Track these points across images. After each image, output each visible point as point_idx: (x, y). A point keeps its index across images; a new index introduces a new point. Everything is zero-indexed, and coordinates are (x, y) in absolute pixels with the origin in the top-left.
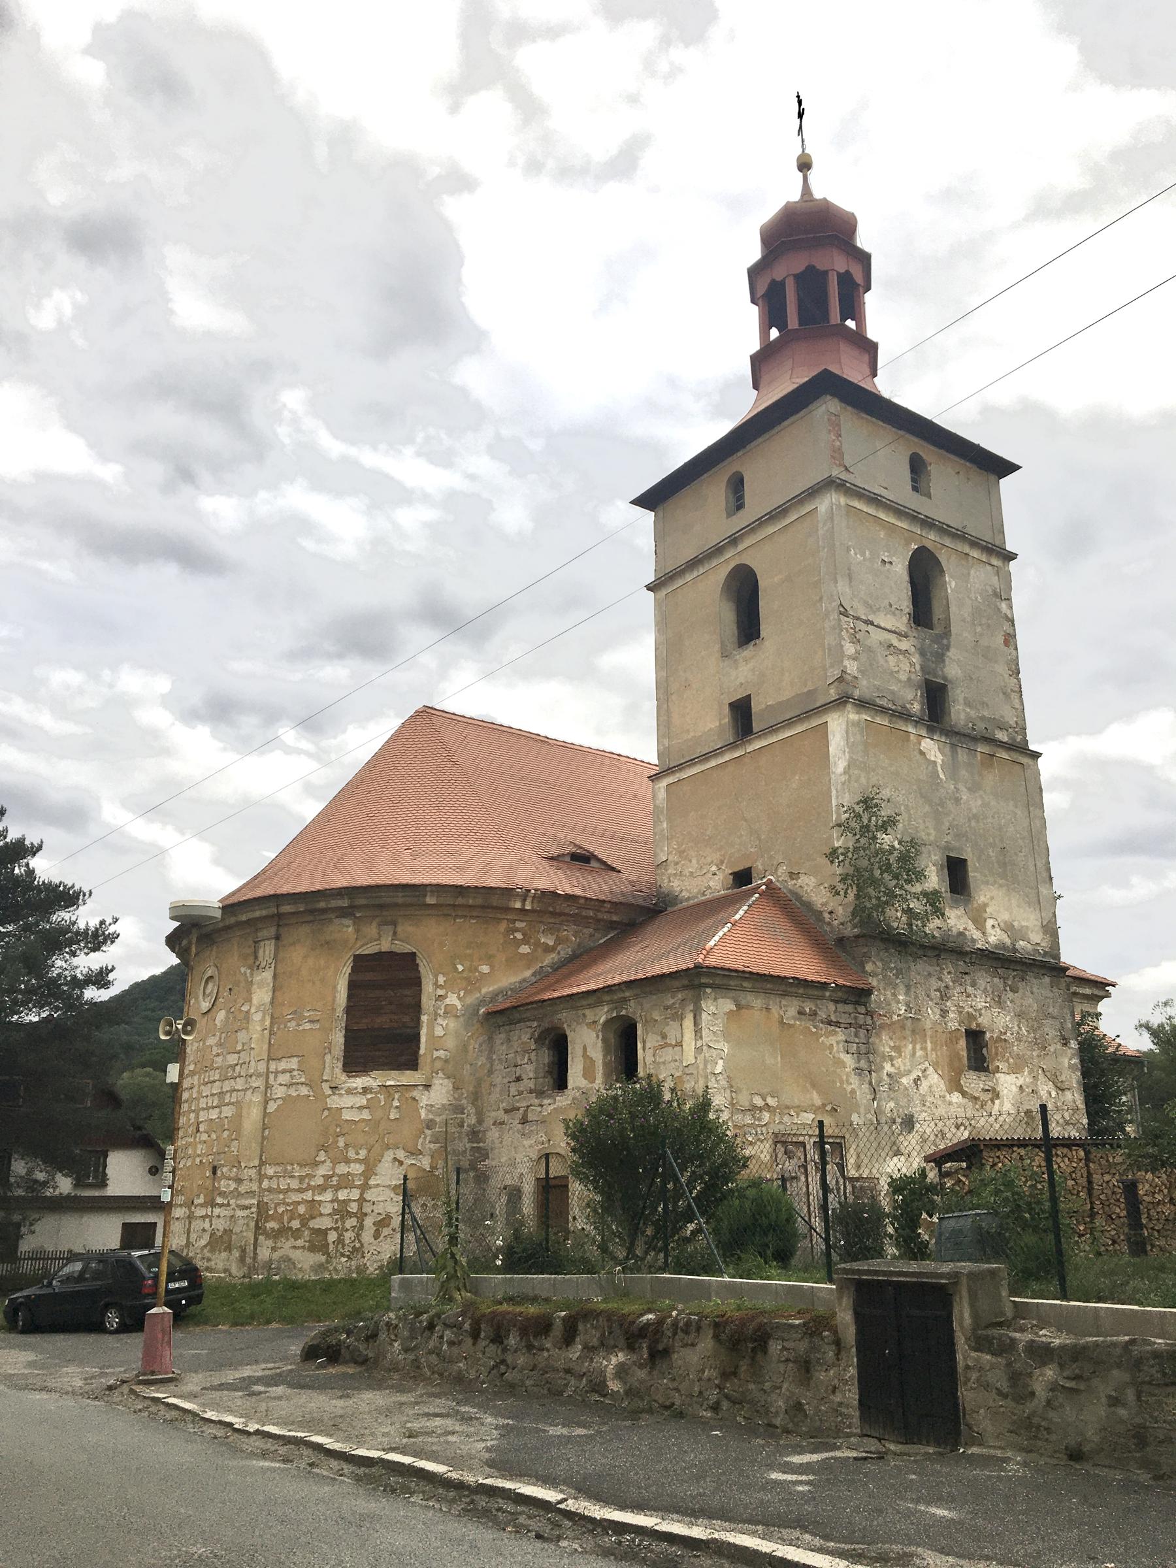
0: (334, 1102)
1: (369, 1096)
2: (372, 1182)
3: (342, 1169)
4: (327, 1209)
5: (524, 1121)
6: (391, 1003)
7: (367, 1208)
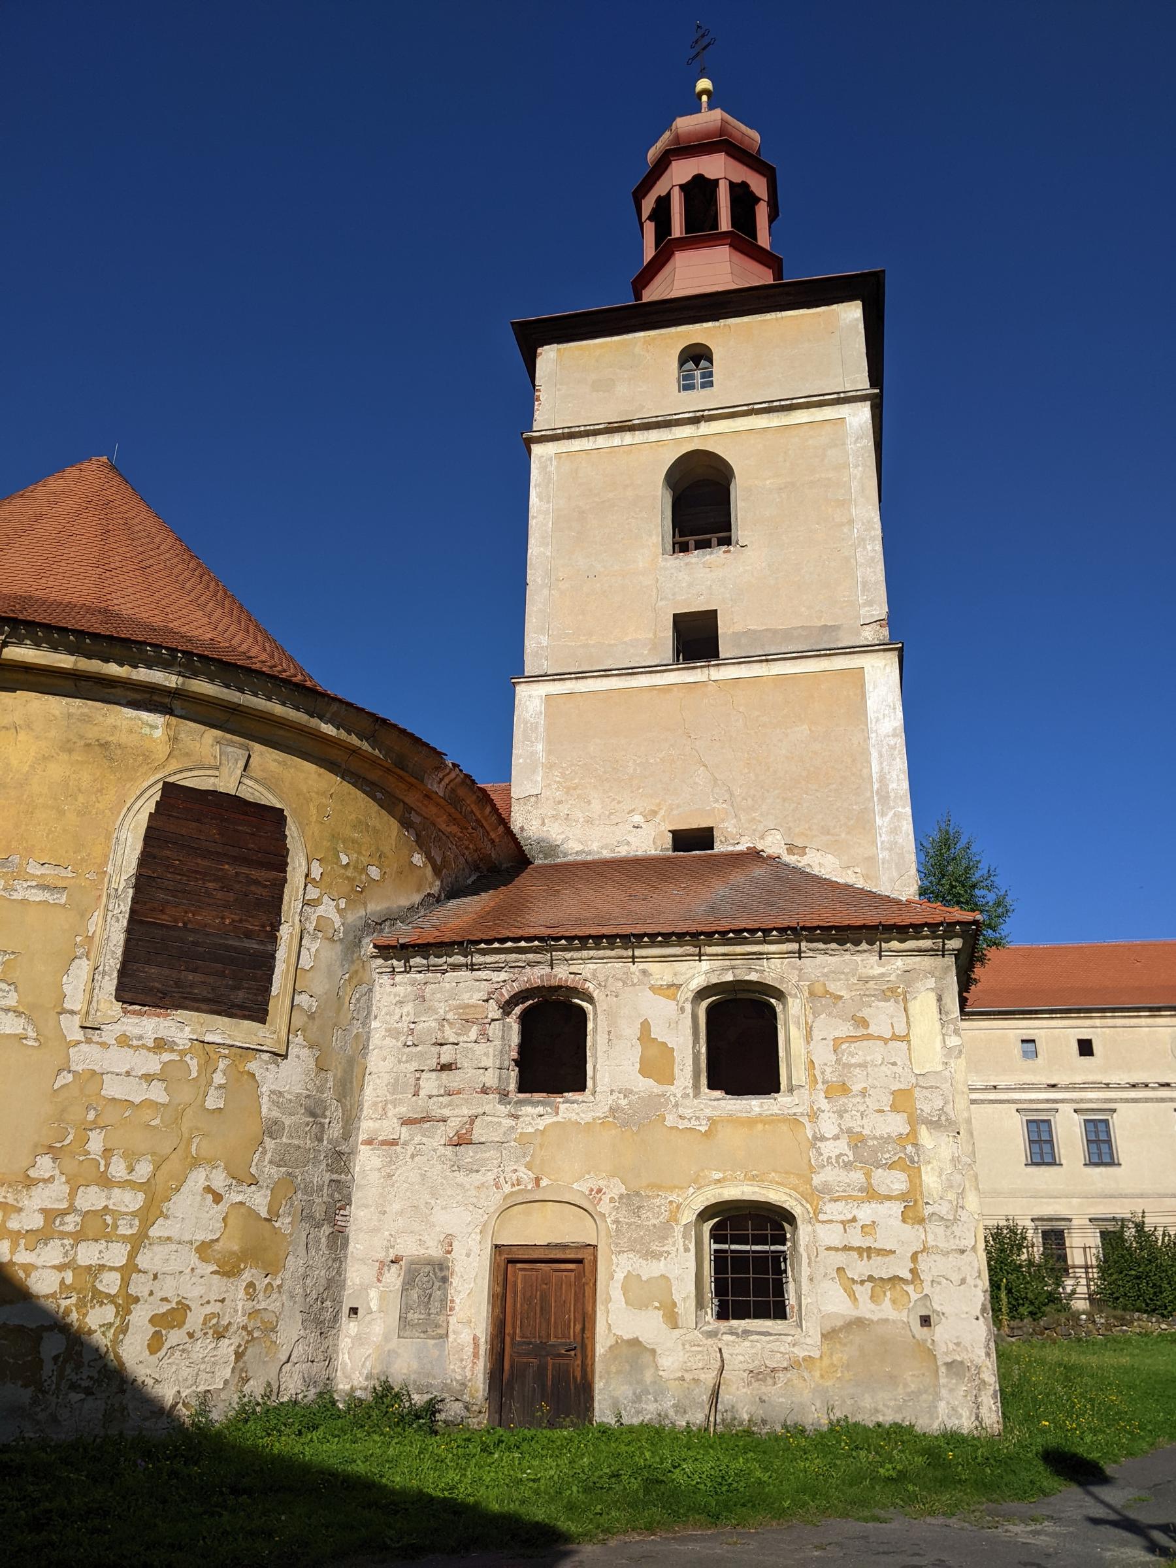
0: (85, 1057)
1: (166, 1057)
2: (154, 1232)
3: (91, 1199)
5: (461, 1141)
7: (139, 1286)
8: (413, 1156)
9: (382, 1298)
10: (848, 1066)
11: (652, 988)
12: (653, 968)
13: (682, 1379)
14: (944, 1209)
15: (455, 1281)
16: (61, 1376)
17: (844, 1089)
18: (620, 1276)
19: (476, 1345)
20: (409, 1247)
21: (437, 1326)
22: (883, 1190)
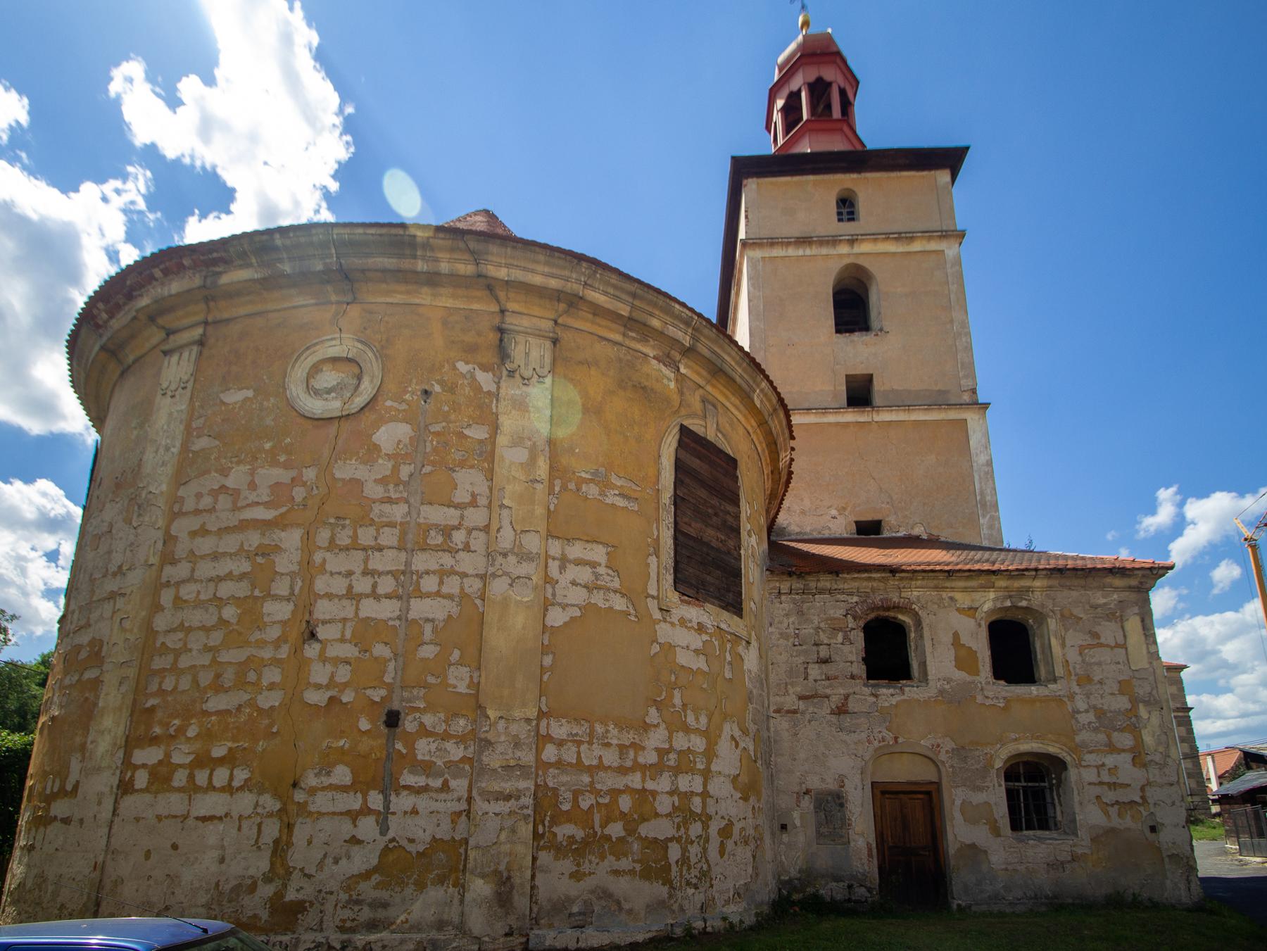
3: (681, 742)
4: (664, 804)
6: (716, 514)
7: (711, 810)
8: (809, 721)
9: (801, 818)
10: (1091, 664)
11: (958, 610)
12: (958, 596)
13: (1006, 869)
14: (1157, 758)
15: (849, 806)
16: (681, 876)
17: (1089, 679)
18: (958, 803)
19: (870, 850)
20: (814, 783)
21: (842, 837)
22: (1119, 745)
